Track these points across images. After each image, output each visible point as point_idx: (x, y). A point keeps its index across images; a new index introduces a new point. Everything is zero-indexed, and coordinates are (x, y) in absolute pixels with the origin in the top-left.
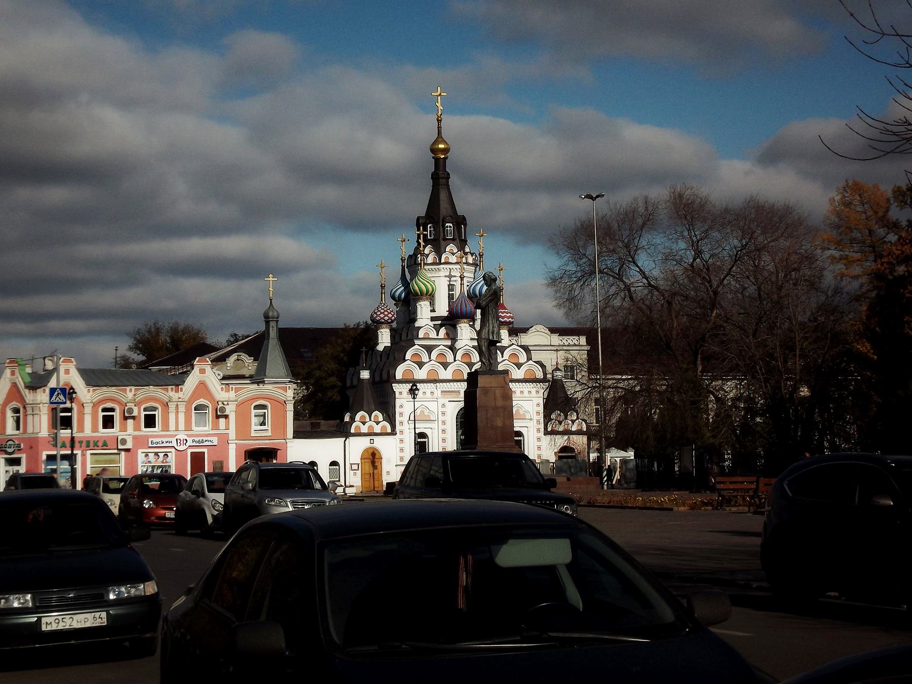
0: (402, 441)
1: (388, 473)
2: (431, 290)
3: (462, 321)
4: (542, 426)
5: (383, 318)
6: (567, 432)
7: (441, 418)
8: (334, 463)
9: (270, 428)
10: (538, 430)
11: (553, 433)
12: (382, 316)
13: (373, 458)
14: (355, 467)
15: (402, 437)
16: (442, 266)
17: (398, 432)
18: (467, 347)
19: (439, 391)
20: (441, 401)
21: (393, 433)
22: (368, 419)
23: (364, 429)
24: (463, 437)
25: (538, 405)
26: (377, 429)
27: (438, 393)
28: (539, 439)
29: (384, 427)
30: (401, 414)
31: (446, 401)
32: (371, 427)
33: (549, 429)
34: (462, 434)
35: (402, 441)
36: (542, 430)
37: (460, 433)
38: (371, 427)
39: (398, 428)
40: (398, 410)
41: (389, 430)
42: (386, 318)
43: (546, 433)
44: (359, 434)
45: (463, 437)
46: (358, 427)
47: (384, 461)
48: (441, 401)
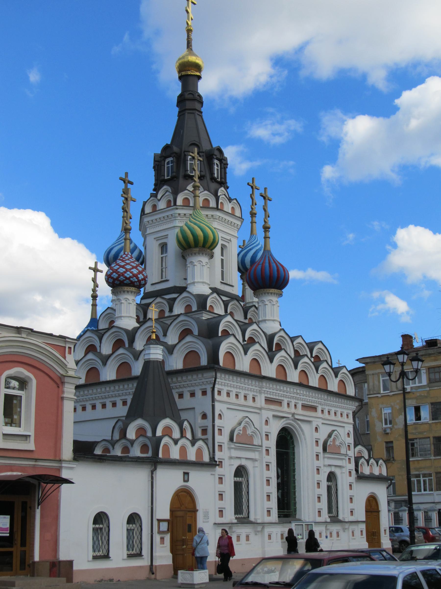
4: (352, 466)
5: (136, 276)
6: (372, 478)
7: (266, 444)
9: (31, 433)
12: (135, 271)
16: (218, 213)
19: (263, 396)
21: (213, 463)
22: (176, 434)
27: (261, 401)
31: (270, 414)
32: (183, 450)
38: (183, 450)
39: (218, 456)
40: (218, 422)
41: (206, 458)
47: (200, 516)
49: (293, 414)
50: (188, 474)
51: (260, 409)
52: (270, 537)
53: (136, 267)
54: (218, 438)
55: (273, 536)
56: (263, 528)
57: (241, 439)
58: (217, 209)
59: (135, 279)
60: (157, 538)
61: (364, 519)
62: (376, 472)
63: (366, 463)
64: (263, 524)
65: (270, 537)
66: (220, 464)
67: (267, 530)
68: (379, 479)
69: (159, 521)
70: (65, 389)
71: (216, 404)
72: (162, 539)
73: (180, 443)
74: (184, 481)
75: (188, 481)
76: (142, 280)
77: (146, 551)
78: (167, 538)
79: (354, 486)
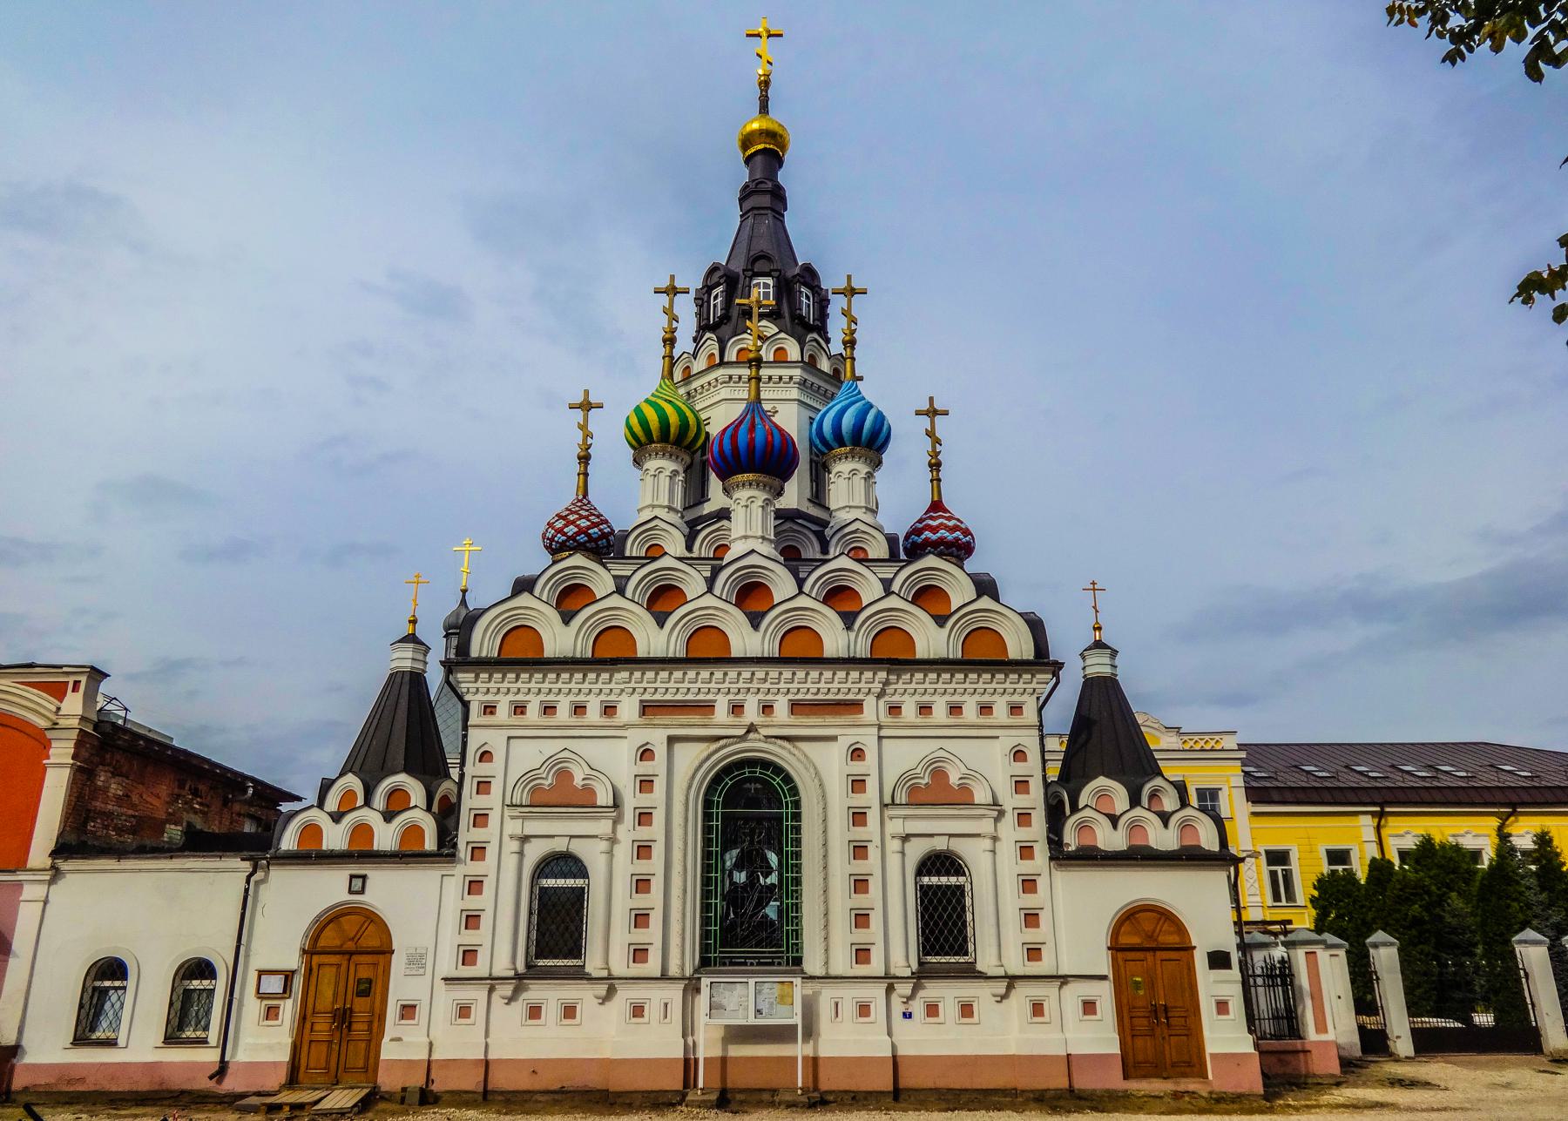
0: (475, 886)
1: (408, 1011)
2: (674, 419)
3: (740, 478)
5: (560, 531)
6: (1140, 857)
8: (201, 968)
10: (1026, 852)
11: (1090, 857)
12: (559, 525)
13: (350, 955)
14: (274, 985)
15: (475, 868)
17: (463, 851)
18: (753, 560)
20: (638, 737)
21: (446, 850)
23: (335, 837)
24: (741, 877)
25: (1019, 755)
26: (386, 837)
27: (628, 709)
28: (1029, 885)
29: (414, 831)
30: (483, 786)
31: (657, 737)
33: (1071, 840)
34: (738, 866)
35: (475, 886)
36: (1042, 851)
37: (731, 857)
38: (363, 831)
39: (467, 834)
40: (473, 769)
41: (430, 844)
42: (571, 530)
43: (1060, 856)
44: (312, 856)
45: (741, 877)
46: (312, 831)
47: (398, 963)
48: (638, 737)
49: (752, 728)
50: (364, 877)
51: (623, 727)
52: (638, 1011)
53: (564, 518)
54: (471, 801)
55: (653, 1011)
56: (611, 991)
57: (559, 794)
58: (722, 363)
59: (560, 538)
60: (251, 1008)
61: (1105, 968)
62: (1163, 839)
63: (1106, 823)
64: (611, 984)
65: (638, 1011)
66: (478, 852)
67: (626, 994)
68: (1189, 857)
69: (261, 973)
70: (52, 751)
71: (471, 731)
72: (271, 1013)
73: (349, 819)
74: (351, 892)
75: (362, 892)
76: (577, 534)
77: (213, 1035)
78: (288, 1009)
79: (1042, 883)
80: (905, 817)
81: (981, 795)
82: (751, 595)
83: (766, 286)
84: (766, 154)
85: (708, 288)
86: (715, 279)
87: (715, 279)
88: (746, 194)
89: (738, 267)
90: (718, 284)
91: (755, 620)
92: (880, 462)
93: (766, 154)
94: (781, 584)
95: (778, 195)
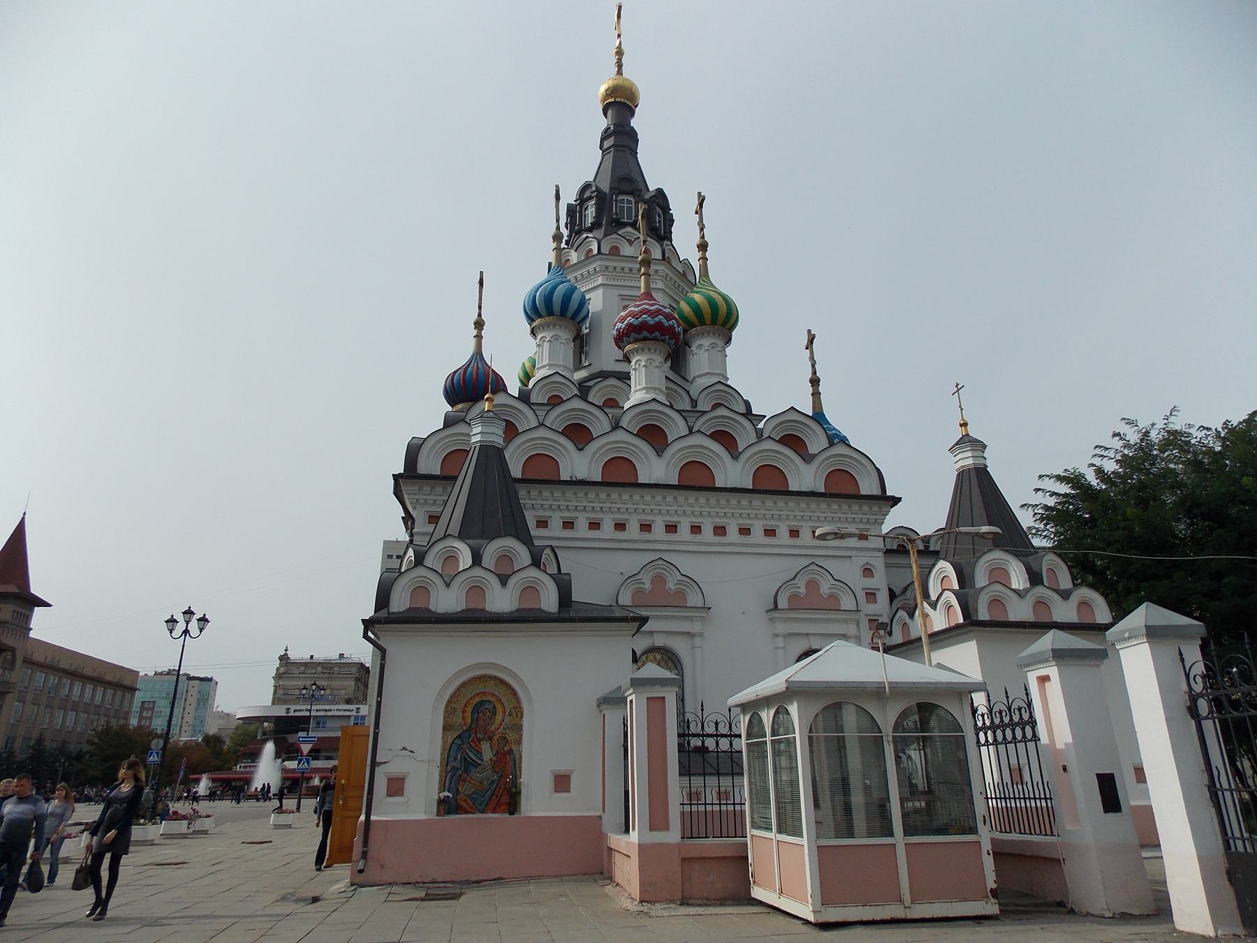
80: (787, 620)
81: (847, 603)
82: (653, 435)
83: (629, 202)
84: (621, 104)
85: (582, 200)
86: (587, 194)
87: (587, 194)
88: (606, 136)
89: (605, 187)
90: (590, 198)
91: (659, 452)
92: (730, 339)
93: (621, 104)
94: (676, 426)
95: (633, 136)
